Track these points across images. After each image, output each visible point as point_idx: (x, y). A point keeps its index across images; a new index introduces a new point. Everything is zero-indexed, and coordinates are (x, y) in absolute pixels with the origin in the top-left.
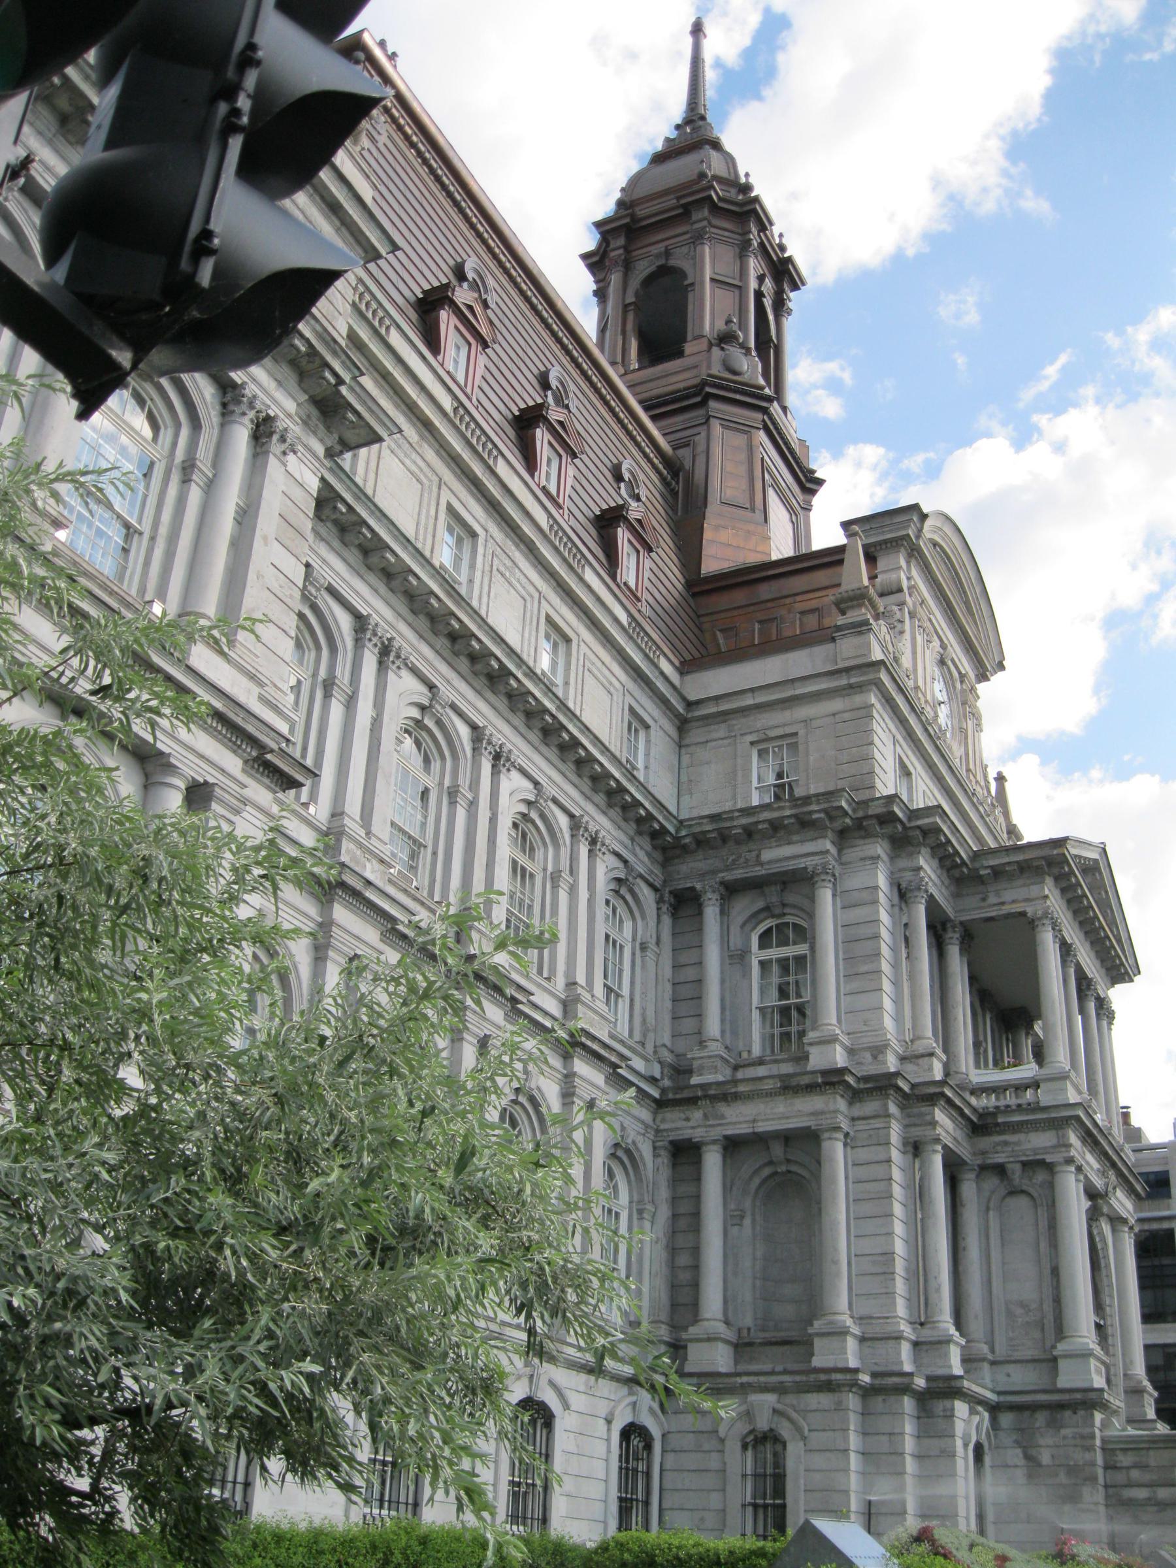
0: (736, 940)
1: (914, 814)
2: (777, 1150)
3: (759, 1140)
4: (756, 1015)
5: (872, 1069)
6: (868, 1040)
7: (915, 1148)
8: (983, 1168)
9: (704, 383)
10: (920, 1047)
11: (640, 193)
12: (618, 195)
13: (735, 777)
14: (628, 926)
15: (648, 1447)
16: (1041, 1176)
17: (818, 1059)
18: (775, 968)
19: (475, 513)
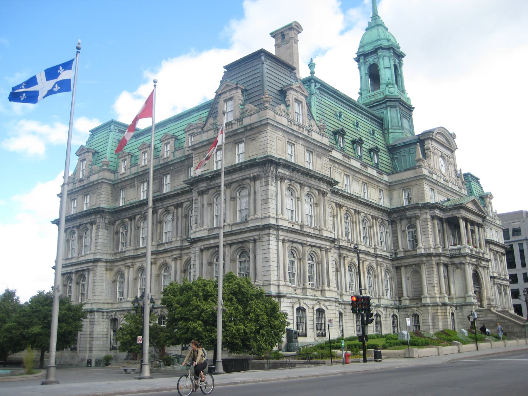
0: (403, 229)
1: (433, 204)
2: (414, 266)
3: (411, 265)
4: (408, 242)
5: (428, 252)
6: (427, 247)
7: (438, 264)
8: (452, 264)
10: (437, 246)
11: (365, 42)
13: (400, 197)
14: (383, 229)
15: (397, 317)
16: (462, 266)
17: (419, 252)
18: (411, 233)
19: (348, 172)
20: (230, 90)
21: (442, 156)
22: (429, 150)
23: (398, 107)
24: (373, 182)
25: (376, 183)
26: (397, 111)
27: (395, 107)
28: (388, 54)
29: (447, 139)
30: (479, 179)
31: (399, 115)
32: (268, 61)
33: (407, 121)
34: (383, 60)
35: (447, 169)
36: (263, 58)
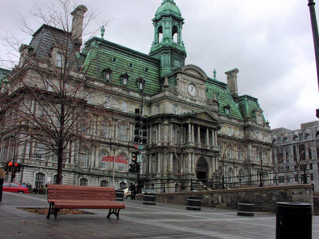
0: (154, 130)
2: (156, 154)
9: (161, 48)
12: (155, 14)
20: (23, 49)
21: (192, 84)
22: (178, 80)
23: (170, 53)
24: (135, 101)
25: (136, 102)
26: (168, 55)
27: (168, 53)
28: (168, 20)
29: (198, 73)
30: (257, 99)
31: (170, 58)
32: (49, 31)
33: (179, 62)
34: (165, 23)
35: (197, 92)
36: (43, 29)
